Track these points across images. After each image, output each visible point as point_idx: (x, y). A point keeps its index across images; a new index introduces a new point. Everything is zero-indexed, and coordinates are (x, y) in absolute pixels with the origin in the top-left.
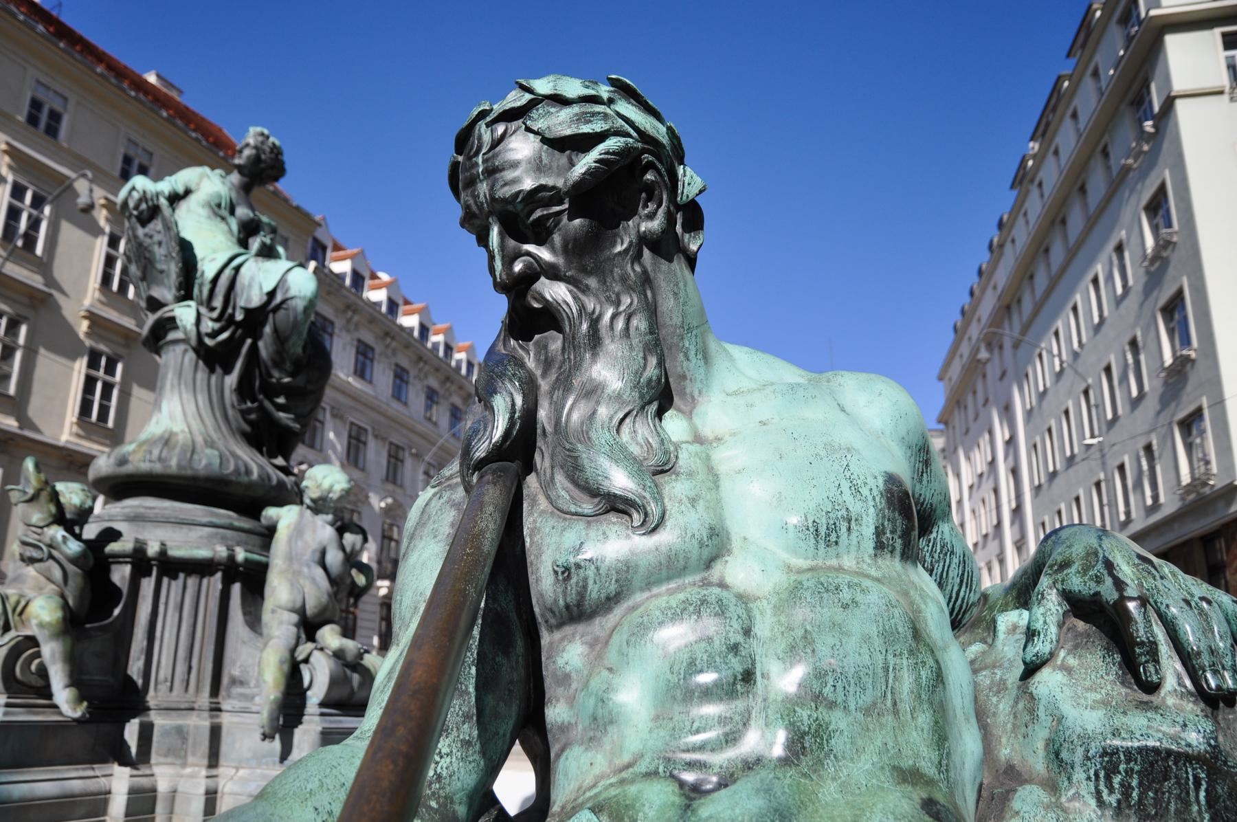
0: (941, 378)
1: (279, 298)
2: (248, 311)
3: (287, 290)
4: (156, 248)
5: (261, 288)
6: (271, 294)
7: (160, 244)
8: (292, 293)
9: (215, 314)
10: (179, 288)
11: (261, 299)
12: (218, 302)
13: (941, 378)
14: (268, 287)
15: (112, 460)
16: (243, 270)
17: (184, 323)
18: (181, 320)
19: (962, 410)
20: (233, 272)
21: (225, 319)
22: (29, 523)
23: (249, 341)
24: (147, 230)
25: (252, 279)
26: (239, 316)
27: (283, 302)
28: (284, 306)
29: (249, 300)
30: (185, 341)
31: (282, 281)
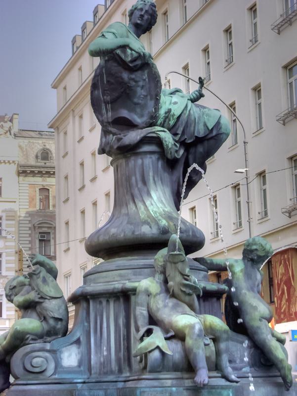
0: (55, 87)
1: (214, 133)
2: (196, 137)
3: (221, 128)
4: (139, 89)
5: (205, 125)
7: (142, 87)
11: (204, 133)
12: (180, 132)
13: (55, 87)
16: (192, 112)
17: (167, 143)
18: (166, 141)
19: (77, 118)
21: (183, 143)
22: (184, 274)
24: (133, 76)
25: (199, 118)
27: (216, 135)
28: (216, 138)
29: (199, 132)
31: (218, 123)
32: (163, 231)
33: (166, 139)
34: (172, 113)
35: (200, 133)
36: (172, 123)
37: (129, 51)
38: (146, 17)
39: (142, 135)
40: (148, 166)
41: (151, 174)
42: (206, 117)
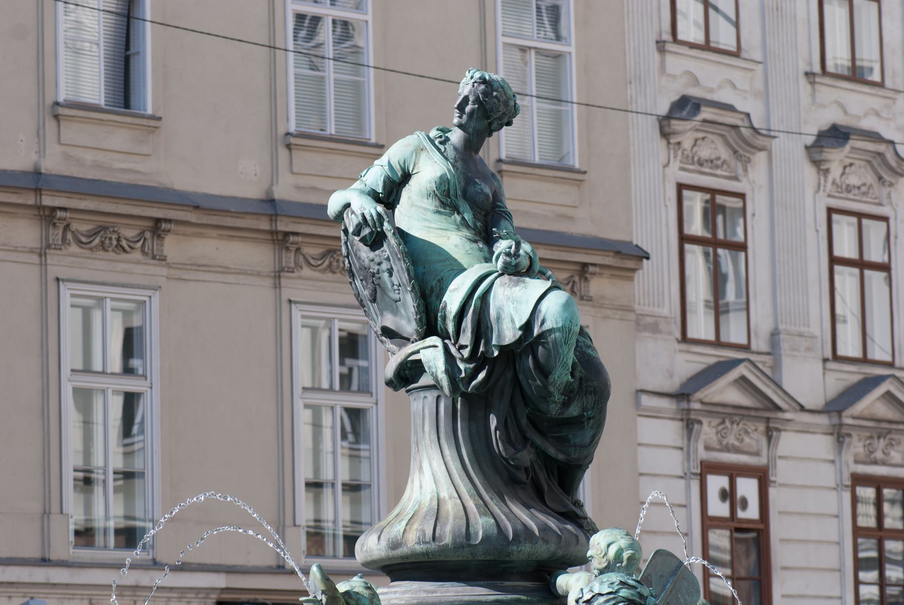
2: (502, 348)
5: (513, 321)
6: (527, 327)
8: (548, 325)
9: (466, 353)
10: (419, 322)
11: (514, 336)
12: (466, 339)
14: (522, 318)
15: (383, 543)
17: (434, 370)
20: (479, 302)
21: (478, 359)
23: (509, 375)
26: (496, 353)
29: (499, 336)
30: (436, 386)
32: (393, 542)
33: (431, 364)
34: (448, 308)
35: (505, 337)
36: (451, 328)
37: (350, 214)
38: (468, 109)
39: (399, 360)
40: (421, 413)
41: (427, 428)
42: (511, 306)
